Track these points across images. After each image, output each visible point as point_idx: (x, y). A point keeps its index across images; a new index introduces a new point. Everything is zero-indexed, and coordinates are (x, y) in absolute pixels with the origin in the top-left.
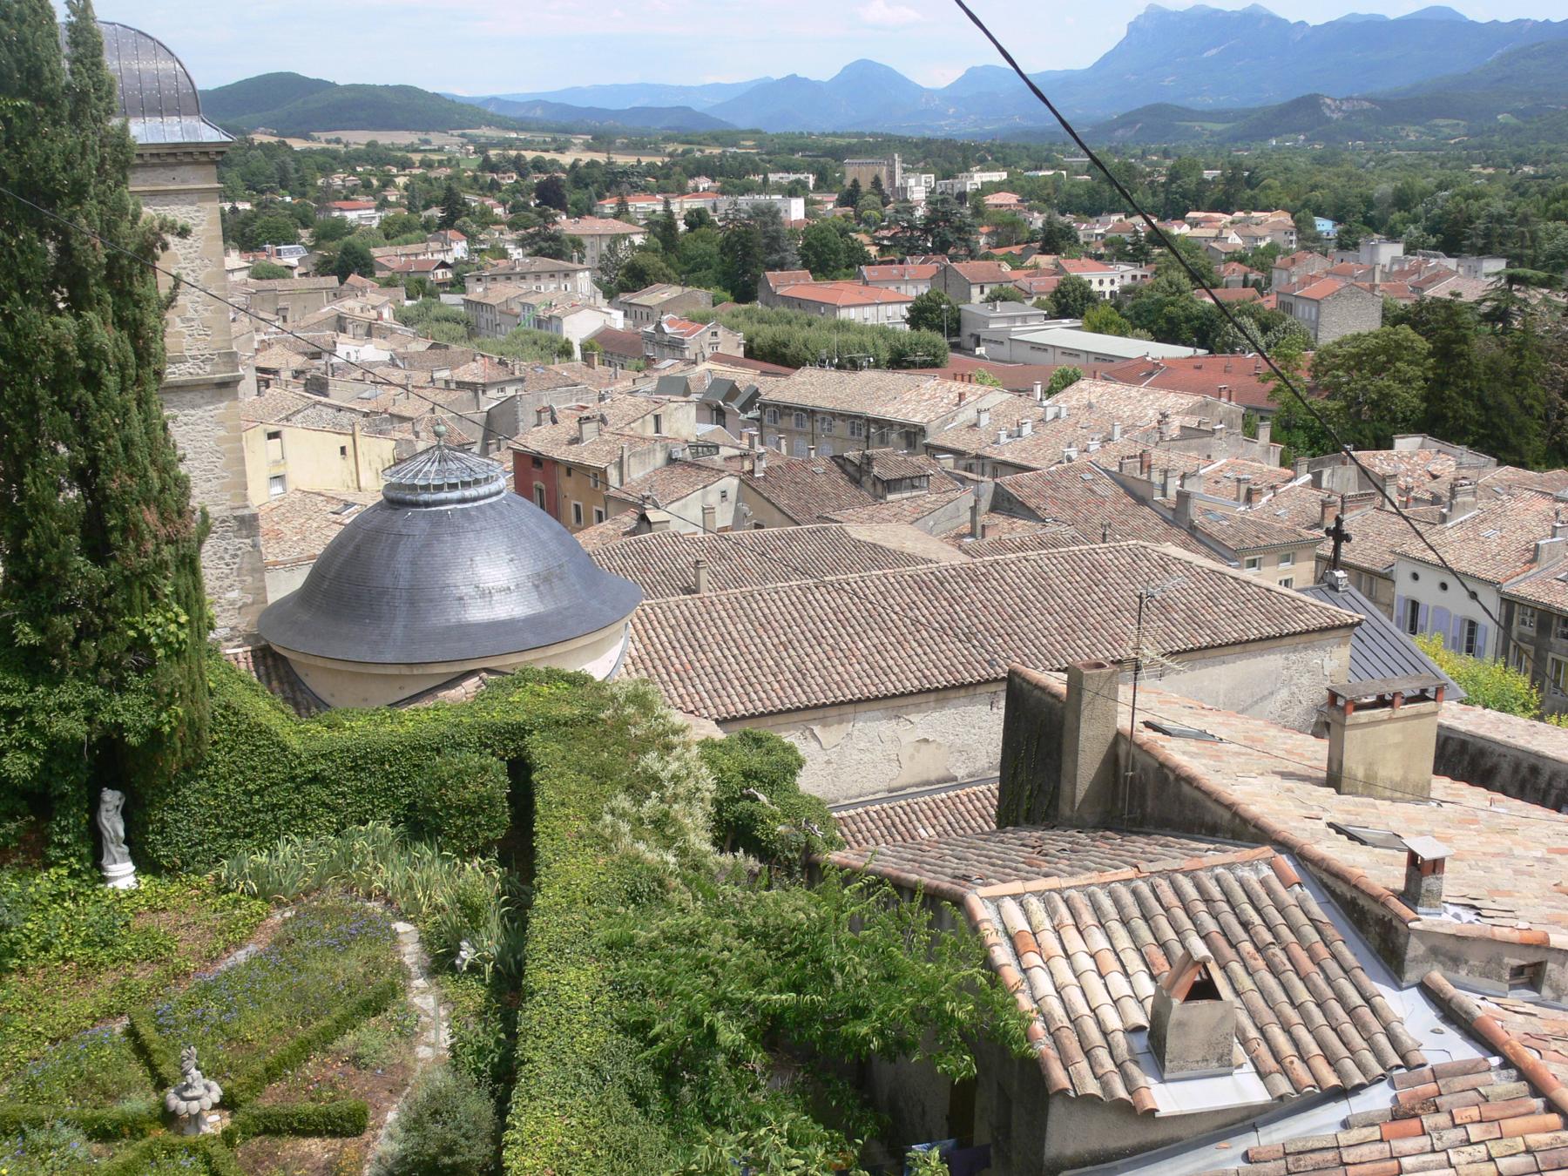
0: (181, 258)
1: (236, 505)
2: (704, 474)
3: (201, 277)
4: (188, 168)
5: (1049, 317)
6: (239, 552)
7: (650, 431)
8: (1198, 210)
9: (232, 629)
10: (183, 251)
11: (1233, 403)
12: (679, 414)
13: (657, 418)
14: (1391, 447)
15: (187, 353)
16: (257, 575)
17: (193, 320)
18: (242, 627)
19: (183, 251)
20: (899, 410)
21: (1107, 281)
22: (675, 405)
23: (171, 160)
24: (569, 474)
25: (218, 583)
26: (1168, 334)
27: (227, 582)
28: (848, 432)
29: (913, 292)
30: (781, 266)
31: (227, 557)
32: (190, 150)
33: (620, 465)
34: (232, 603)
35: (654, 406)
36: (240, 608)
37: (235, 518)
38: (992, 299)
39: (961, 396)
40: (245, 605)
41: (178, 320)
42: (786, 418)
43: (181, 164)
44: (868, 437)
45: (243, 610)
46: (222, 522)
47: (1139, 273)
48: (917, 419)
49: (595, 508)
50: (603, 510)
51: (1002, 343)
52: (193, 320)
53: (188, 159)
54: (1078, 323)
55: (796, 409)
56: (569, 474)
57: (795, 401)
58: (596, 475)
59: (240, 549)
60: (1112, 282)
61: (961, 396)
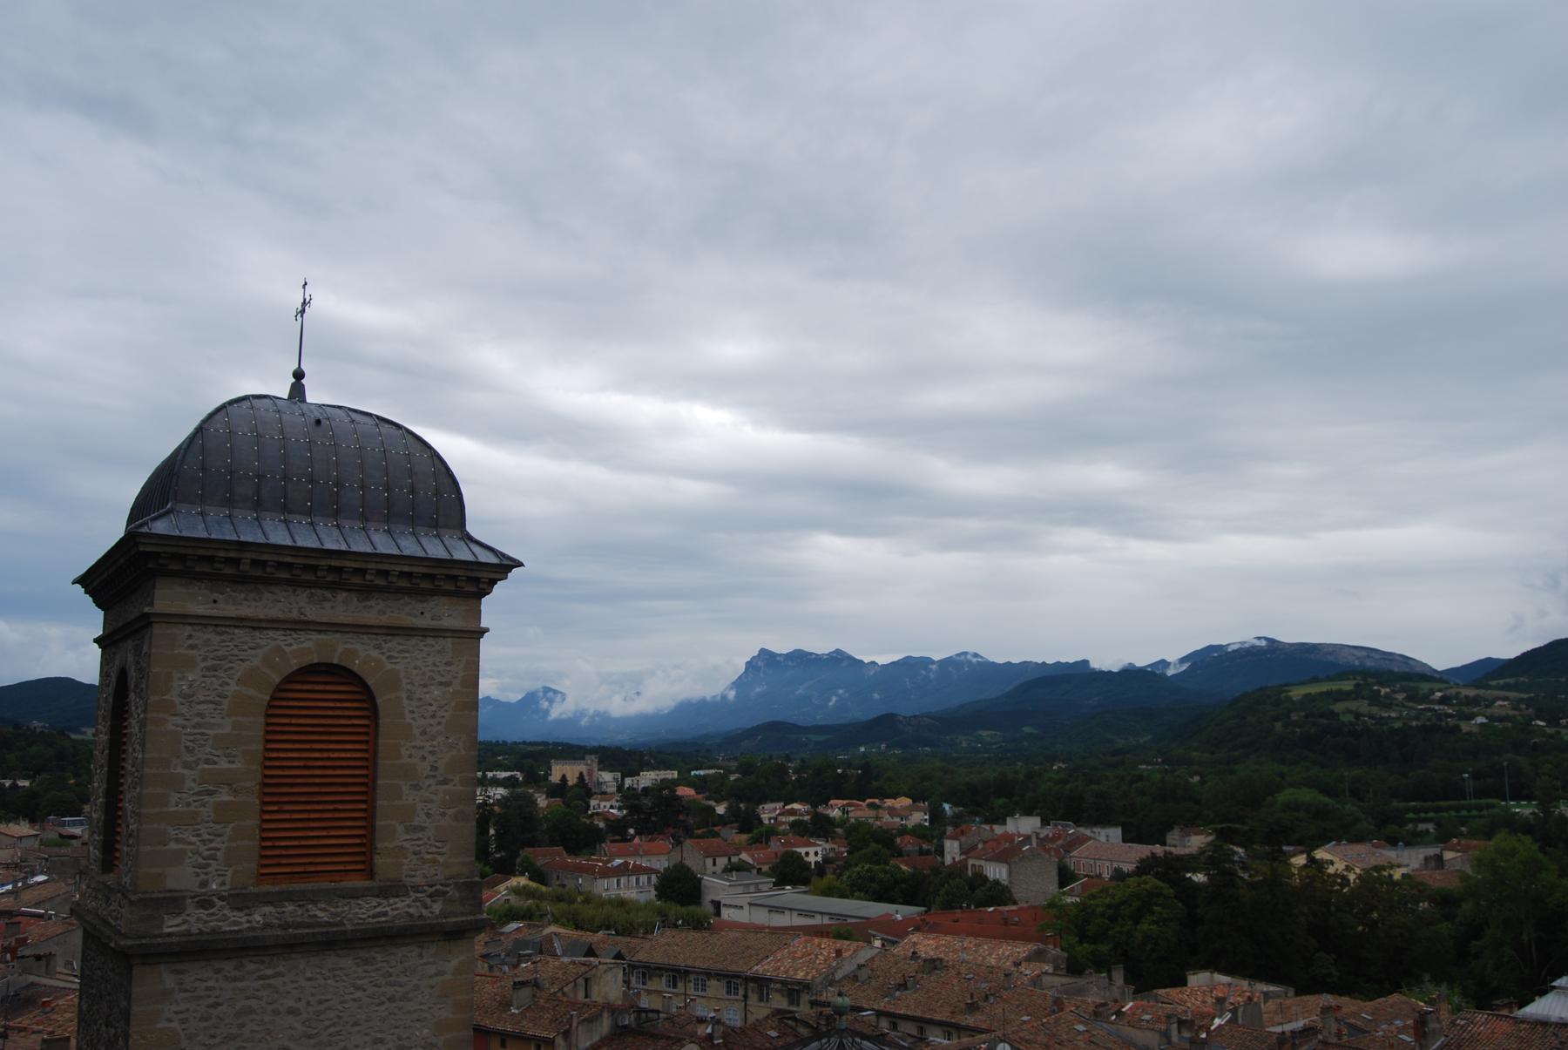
0: (416, 732)
4: (444, 600)
5: (775, 884)
7: (581, 996)
8: (838, 798)
11: (1058, 949)
12: (609, 976)
13: (587, 980)
14: (1185, 984)
15: (408, 881)
17: (422, 829)
22: (605, 967)
23: (425, 585)
24: (503, 1045)
29: (661, 863)
30: (532, 843)
32: (455, 572)
33: (566, 1035)
35: (584, 969)
38: (729, 869)
39: (839, 952)
41: (400, 828)
44: (746, 997)
47: (827, 846)
48: (800, 975)
51: (741, 907)
52: (422, 829)
54: (803, 888)
55: (667, 970)
56: (503, 1045)
57: (666, 961)
60: (816, 854)
61: (839, 952)
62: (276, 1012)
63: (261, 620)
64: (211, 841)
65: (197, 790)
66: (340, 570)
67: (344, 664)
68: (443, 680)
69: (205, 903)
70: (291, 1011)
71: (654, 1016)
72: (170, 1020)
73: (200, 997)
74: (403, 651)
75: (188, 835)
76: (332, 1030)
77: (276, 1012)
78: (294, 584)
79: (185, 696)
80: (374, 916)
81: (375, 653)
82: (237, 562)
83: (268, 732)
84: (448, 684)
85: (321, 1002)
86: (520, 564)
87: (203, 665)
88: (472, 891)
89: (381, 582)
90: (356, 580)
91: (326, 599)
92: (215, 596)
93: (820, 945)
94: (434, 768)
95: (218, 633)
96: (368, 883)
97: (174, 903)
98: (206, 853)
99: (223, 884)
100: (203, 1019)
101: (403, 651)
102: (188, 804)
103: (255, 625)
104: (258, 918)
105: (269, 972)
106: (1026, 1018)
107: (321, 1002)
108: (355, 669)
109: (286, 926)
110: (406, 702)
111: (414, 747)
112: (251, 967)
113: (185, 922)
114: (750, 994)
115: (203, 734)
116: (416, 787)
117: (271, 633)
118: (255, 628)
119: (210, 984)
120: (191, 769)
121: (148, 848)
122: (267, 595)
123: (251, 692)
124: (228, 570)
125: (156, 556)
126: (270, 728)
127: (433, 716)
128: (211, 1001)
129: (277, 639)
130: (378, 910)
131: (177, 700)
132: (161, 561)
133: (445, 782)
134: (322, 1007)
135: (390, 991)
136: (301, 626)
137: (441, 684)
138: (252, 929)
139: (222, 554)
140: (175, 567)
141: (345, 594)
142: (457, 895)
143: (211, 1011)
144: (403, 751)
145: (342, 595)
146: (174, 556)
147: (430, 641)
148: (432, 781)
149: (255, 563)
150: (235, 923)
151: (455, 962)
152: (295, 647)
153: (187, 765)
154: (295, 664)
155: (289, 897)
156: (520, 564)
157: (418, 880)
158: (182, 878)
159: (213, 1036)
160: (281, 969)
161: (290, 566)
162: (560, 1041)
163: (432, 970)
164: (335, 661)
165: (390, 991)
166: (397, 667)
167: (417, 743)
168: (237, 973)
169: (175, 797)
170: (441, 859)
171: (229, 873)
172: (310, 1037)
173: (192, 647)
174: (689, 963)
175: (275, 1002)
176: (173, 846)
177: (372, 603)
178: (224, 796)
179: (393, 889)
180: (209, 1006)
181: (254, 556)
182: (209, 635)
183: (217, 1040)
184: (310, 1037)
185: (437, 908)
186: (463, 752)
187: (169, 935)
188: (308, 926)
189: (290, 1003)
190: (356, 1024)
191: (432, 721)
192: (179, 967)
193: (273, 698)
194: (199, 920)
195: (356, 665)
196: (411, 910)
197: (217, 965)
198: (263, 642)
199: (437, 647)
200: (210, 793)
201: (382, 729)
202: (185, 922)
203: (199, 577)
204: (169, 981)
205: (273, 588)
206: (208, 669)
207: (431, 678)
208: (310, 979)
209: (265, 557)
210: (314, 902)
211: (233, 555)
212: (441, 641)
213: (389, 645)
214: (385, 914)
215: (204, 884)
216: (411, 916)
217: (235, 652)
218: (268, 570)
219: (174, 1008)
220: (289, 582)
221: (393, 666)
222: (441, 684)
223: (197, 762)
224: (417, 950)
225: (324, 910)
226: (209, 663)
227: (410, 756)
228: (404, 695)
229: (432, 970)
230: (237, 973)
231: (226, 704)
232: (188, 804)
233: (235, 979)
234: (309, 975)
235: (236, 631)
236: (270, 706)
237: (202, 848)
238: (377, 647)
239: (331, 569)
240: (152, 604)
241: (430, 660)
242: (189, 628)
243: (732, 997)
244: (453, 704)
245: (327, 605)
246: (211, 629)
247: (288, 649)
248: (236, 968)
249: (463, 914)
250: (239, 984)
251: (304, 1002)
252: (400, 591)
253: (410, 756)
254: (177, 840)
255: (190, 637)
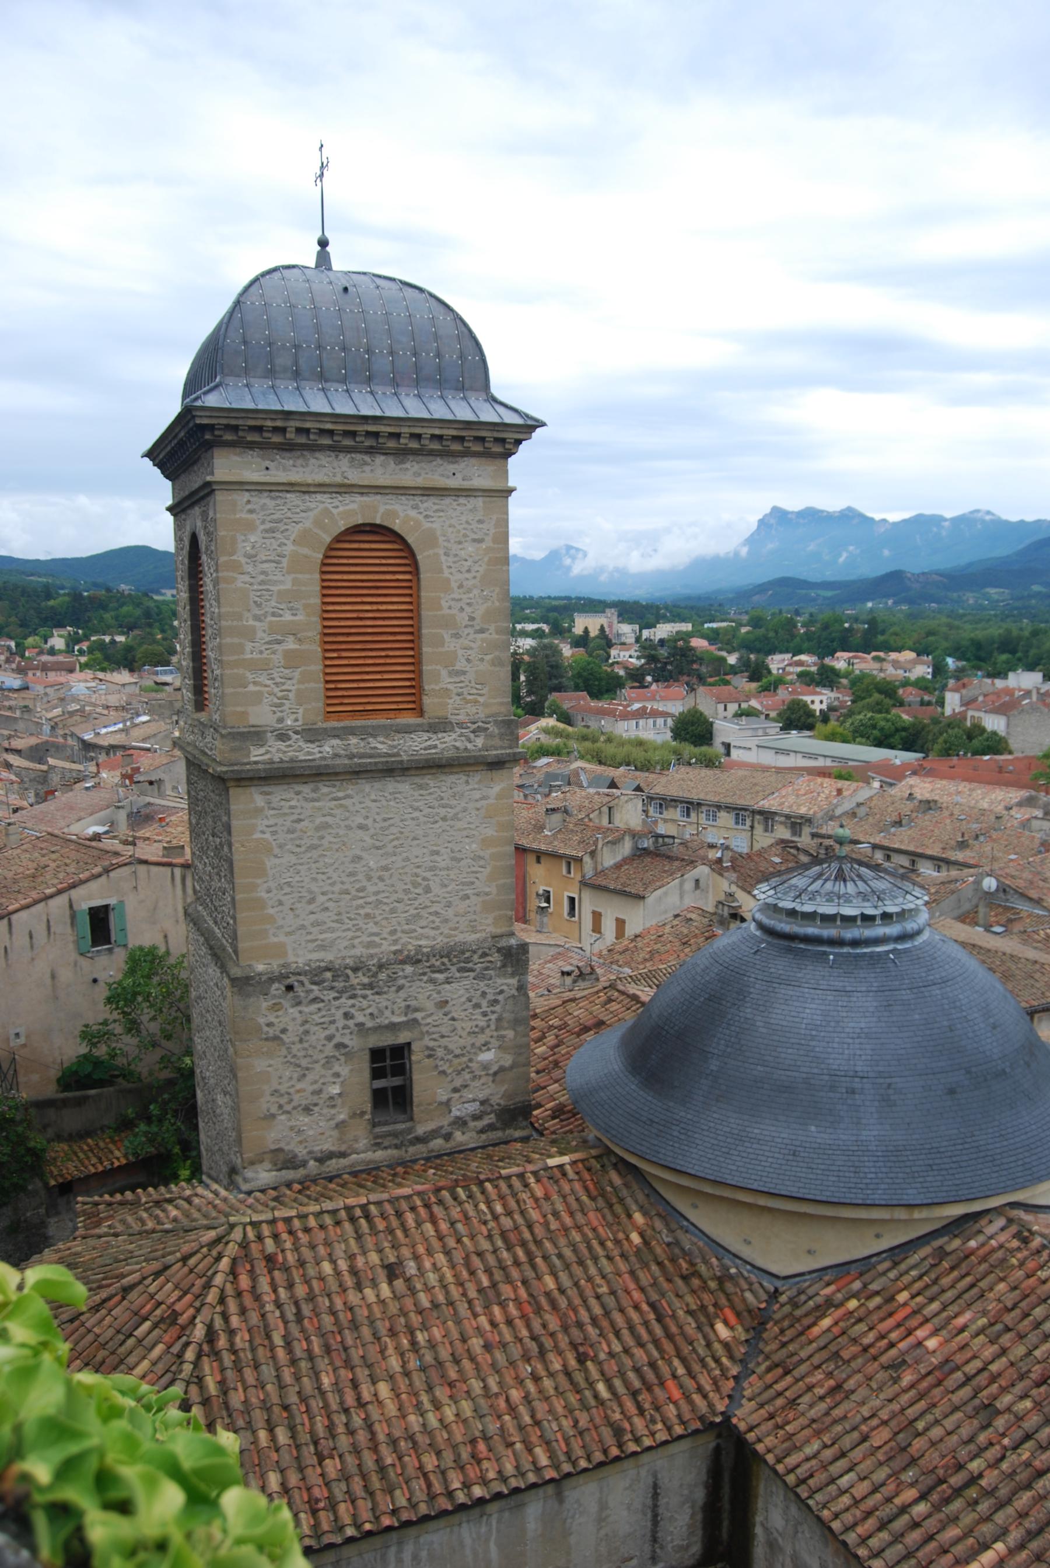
1: (499, 931)
2: (677, 863)
3: (478, 615)
4: (473, 461)
5: (782, 729)
6: (500, 998)
7: (605, 822)
9: (483, 1103)
10: (459, 576)
12: (630, 805)
15: (453, 719)
16: (520, 1029)
17: (464, 673)
18: (495, 1100)
19: (459, 576)
20: (782, 804)
21: (817, 702)
23: (456, 447)
24: (538, 861)
25: (471, 1040)
26: (880, 743)
27: (482, 1039)
28: (733, 822)
29: (676, 709)
30: (559, 688)
31: (484, 1003)
32: (483, 434)
33: (593, 854)
34: (485, 1067)
35: (607, 799)
36: (495, 1074)
37: (499, 950)
39: (839, 792)
40: (502, 1069)
41: (444, 673)
42: (671, 810)
43: (466, 454)
44: (752, 827)
45: (498, 1077)
46: (481, 957)
47: (833, 695)
48: (803, 810)
49: (567, 894)
50: (576, 896)
53: (477, 448)
54: (808, 733)
55: (681, 802)
56: (538, 861)
57: (681, 794)
58: (569, 864)
59: (502, 992)
61: (839, 792)
62: (349, 828)
63: (309, 485)
64: (283, 684)
65: (268, 639)
66: (376, 435)
67: (385, 524)
68: (476, 537)
69: (283, 737)
70: (361, 827)
71: (671, 841)
72: (263, 832)
73: (285, 814)
74: (437, 511)
75: (263, 679)
76: (396, 843)
77: (349, 828)
78: (336, 449)
79: (249, 557)
80: (425, 749)
81: (413, 513)
82: (283, 430)
83: (323, 587)
84: (480, 541)
85: (385, 820)
86: (543, 424)
87: (262, 527)
88: (510, 728)
89: (414, 445)
90: (392, 444)
91: (366, 464)
92: (267, 463)
93: (822, 784)
94: (472, 619)
95: (272, 498)
96: (419, 720)
97: (256, 736)
98: (280, 694)
99: (296, 720)
100: (290, 831)
101: (437, 511)
102: (261, 652)
103: (304, 489)
104: (328, 749)
105: (341, 794)
106: (1013, 857)
107: (385, 820)
108: (396, 528)
109: (351, 756)
110: (443, 558)
111: (453, 599)
112: (325, 790)
113: (267, 752)
114: (756, 825)
115: (268, 590)
116: (457, 636)
117: (319, 497)
118: (304, 492)
119: (293, 803)
120: (260, 621)
121: (232, 690)
122: (312, 461)
123: (305, 551)
124: (277, 439)
125: (211, 427)
126: (326, 584)
127: (469, 571)
128: (295, 817)
129: (322, 502)
130: (429, 743)
131: (243, 560)
132: (217, 433)
133: (482, 631)
134: (386, 824)
135: (443, 812)
136: (345, 489)
137: (474, 540)
138: (324, 758)
139: (269, 423)
140: (229, 437)
141: (382, 458)
142: (496, 731)
143: (296, 825)
144: (443, 603)
145: (380, 459)
146: (228, 427)
147: (462, 500)
148: (470, 630)
149: (299, 431)
150: (309, 753)
151: (497, 789)
152: (341, 509)
153: (257, 618)
154: (342, 525)
155: (352, 731)
156: (543, 424)
157: (462, 718)
158: (262, 715)
159: (299, 846)
160: (350, 792)
161: (331, 433)
162: (587, 859)
163: (477, 795)
164: (378, 522)
165: (443, 812)
166: (434, 526)
167: (456, 596)
168: (315, 795)
169: (249, 646)
170: (481, 699)
171: (301, 711)
172: (378, 848)
173: (251, 511)
174: (702, 796)
175: (347, 819)
176: (252, 688)
177: (408, 465)
178: (291, 645)
179: (440, 726)
180: (293, 822)
181: (298, 424)
182: (265, 500)
183: (303, 849)
184: (378, 848)
185: (480, 742)
186: (497, 604)
187: (256, 763)
188: (371, 756)
189: (360, 820)
190: (415, 839)
191: (467, 575)
192: (266, 789)
193: (326, 557)
194: (279, 750)
195: (397, 525)
196: (458, 744)
197: (298, 788)
198: (312, 505)
199: (469, 506)
200: (279, 642)
201: (423, 583)
202: (267, 752)
203: (251, 446)
204: (259, 800)
205: (318, 455)
206: (266, 531)
207: (465, 536)
208: (375, 801)
209: (308, 425)
210: (374, 736)
211: (279, 423)
212: (472, 500)
213: (425, 505)
214: (435, 747)
215: (281, 720)
216: (457, 748)
217: (289, 514)
218: (312, 437)
219: (266, 822)
220: (332, 448)
221: (429, 525)
222: (474, 540)
223: (265, 615)
224: (464, 778)
225: (383, 743)
226: (268, 526)
227: (450, 608)
228: (441, 552)
229: (477, 795)
230: (315, 795)
231: (285, 562)
232: (261, 652)
233: (314, 800)
234: (373, 797)
235: (288, 495)
236: (324, 564)
237: (276, 690)
238: (415, 507)
239: (369, 434)
240: (212, 474)
241: (464, 518)
242: (247, 494)
243: (740, 827)
244: (486, 559)
245: (367, 468)
246: (266, 494)
247: (335, 511)
248: (314, 791)
249: (502, 748)
250: (317, 804)
251: (370, 820)
252: (432, 453)
253: (450, 608)
254: (255, 683)
255: (249, 502)
